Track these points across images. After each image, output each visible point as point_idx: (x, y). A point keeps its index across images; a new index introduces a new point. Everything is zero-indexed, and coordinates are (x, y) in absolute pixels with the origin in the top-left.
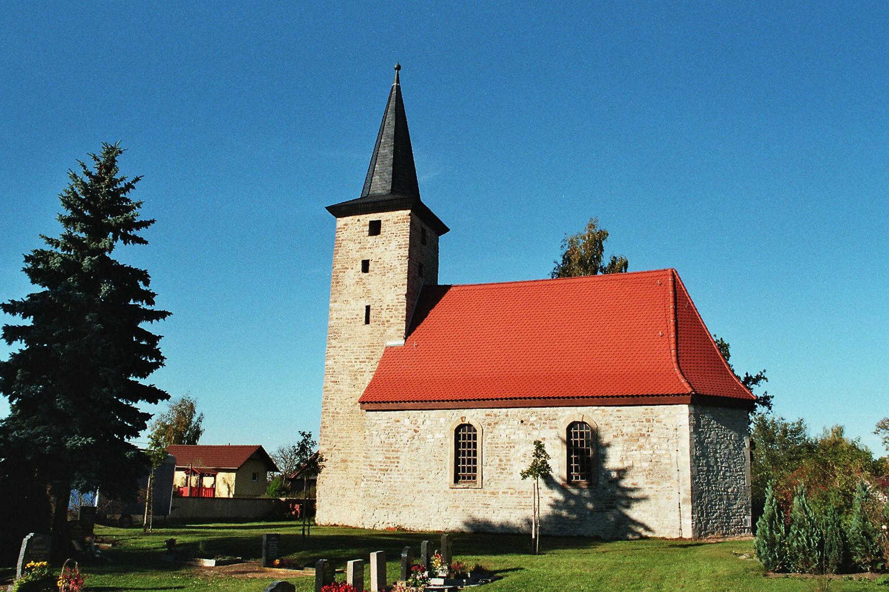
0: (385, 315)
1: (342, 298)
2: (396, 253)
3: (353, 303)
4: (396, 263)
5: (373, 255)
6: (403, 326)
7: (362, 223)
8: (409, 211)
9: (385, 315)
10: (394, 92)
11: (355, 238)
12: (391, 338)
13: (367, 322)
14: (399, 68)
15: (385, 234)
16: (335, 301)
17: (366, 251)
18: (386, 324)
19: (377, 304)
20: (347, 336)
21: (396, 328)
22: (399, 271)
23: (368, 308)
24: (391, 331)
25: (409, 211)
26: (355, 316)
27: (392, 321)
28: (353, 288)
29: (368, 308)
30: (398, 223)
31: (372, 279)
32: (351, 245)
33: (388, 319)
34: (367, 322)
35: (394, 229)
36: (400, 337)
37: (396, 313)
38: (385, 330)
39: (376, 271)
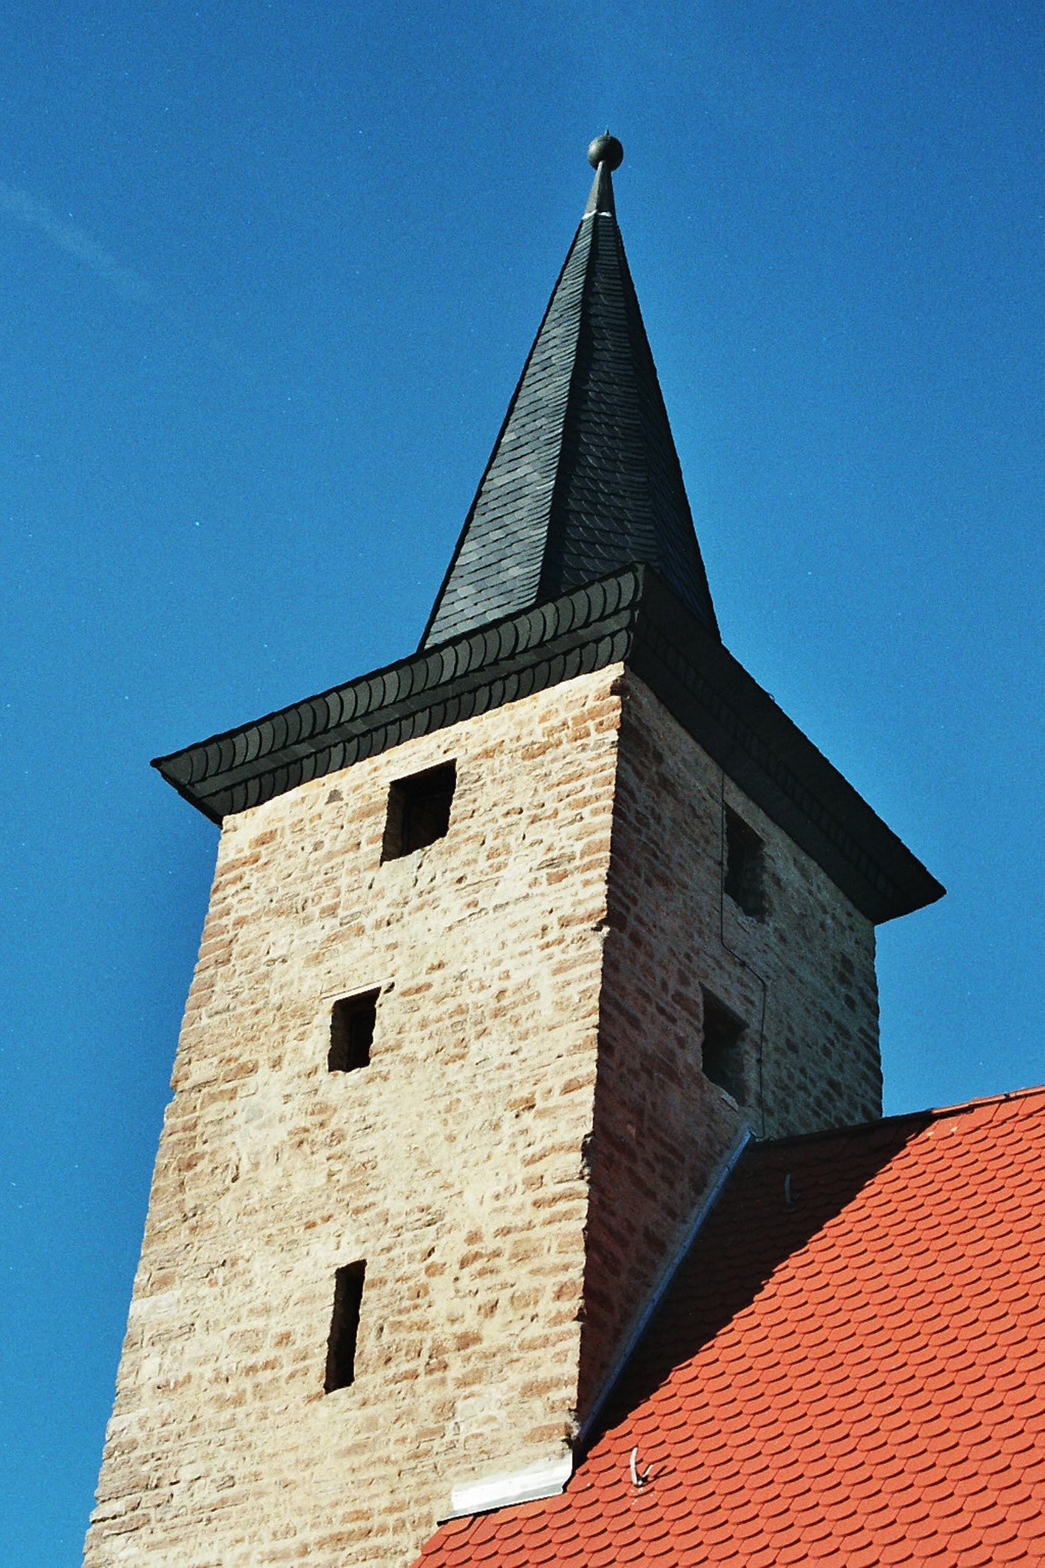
0: (448, 1304)
1: (208, 1252)
2: (531, 914)
3: (262, 1266)
4: (534, 969)
5: (400, 958)
6: (562, 1362)
7: (352, 802)
8: (615, 671)
9: (448, 1304)
10: (585, 242)
11: (304, 890)
12: (483, 1457)
13: (340, 1371)
14: (611, 154)
15: (475, 825)
16: (165, 1282)
17: (363, 944)
18: (457, 1368)
19: (410, 1245)
20: (206, 1494)
21: (517, 1377)
22: (546, 1010)
23: (351, 1281)
24: (486, 1407)
25: (615, 671)
26: (267, 1353)
27: (493, 1333)
28: (270, 1176)
29: (351, 1281)
30: (546, 759)
31: (389, 1092)
32: (282, 936)
33: (471, 1323)
34: (340, 1371)
35: (524, 782)
36: (540, 1435)
37: (522, 1278)
38: (446, 1409)
39: (416, 1044)
